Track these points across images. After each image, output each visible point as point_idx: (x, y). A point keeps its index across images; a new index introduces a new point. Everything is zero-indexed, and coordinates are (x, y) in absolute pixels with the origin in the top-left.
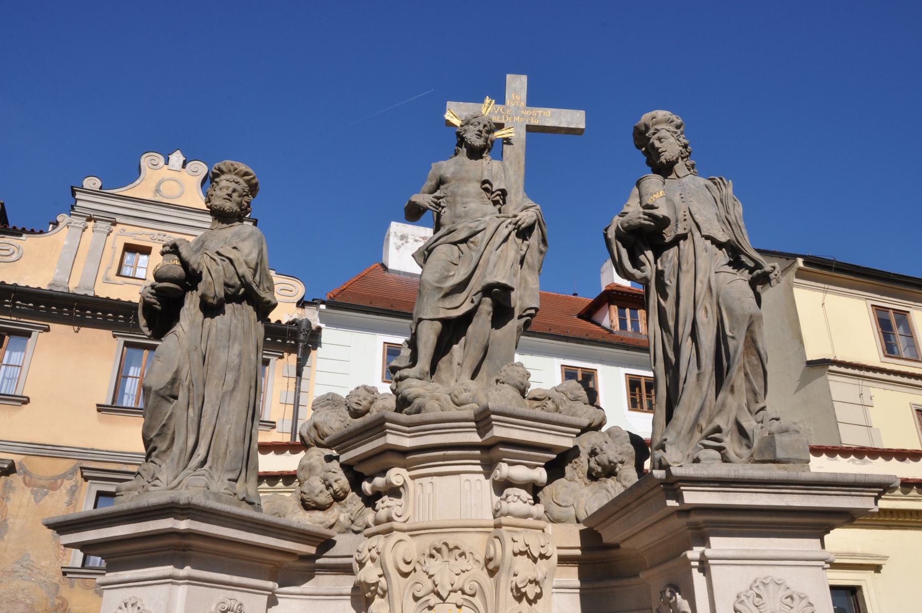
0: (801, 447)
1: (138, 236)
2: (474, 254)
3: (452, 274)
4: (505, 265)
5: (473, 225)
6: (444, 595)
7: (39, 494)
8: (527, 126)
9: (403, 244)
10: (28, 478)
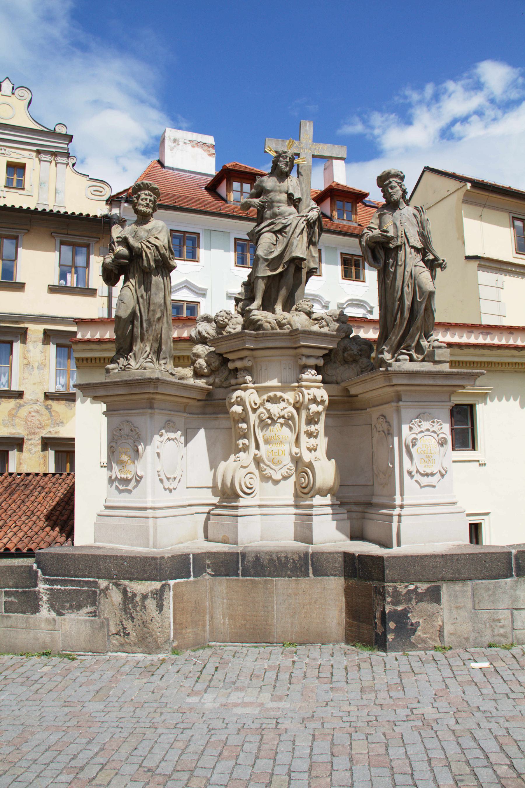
2: (285, 239)
3: (273, 250)
4: (302, 246)
5: (284, 221)
6: (276, 419)
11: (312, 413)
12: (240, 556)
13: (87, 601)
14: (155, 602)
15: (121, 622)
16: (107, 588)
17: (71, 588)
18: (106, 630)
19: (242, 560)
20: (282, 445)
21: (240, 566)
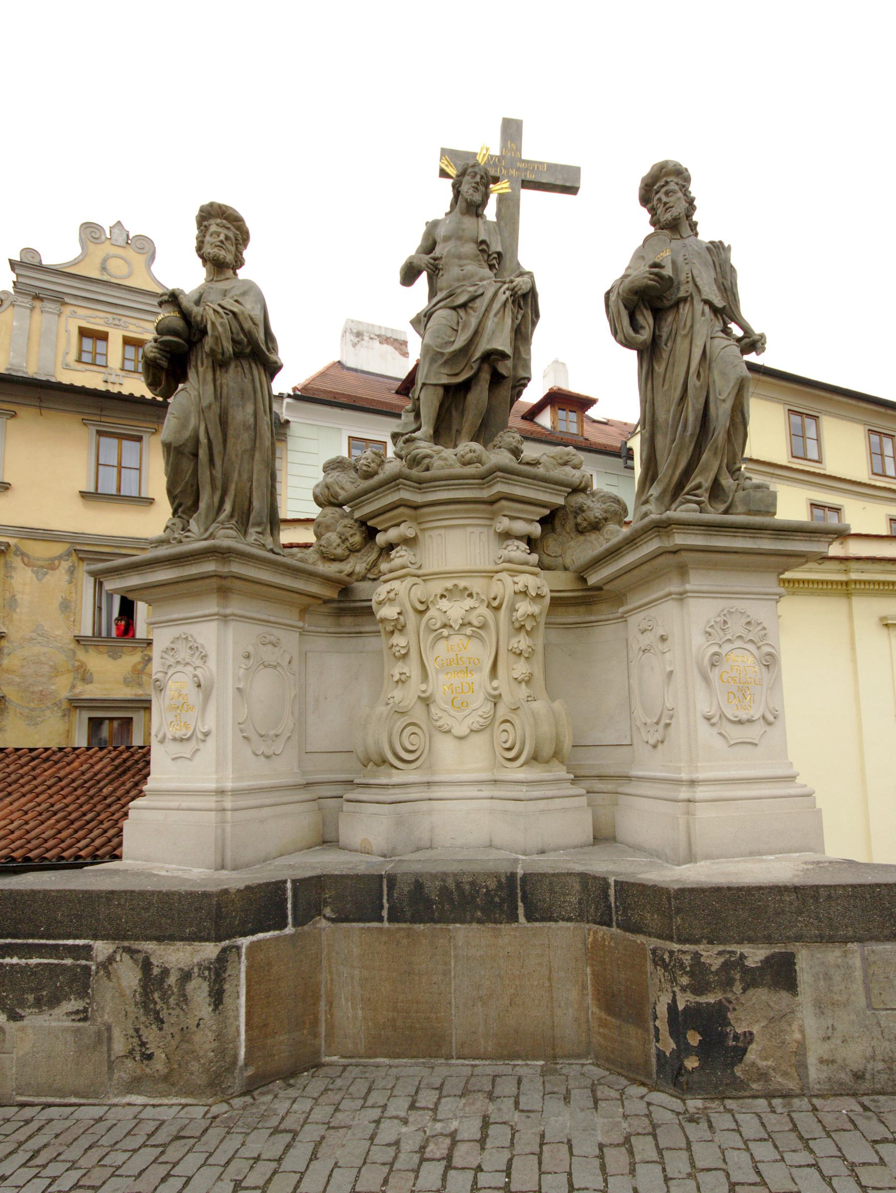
8: (523, 181)
10: (26, 559)
11: (523, 616)
12: (385, 881)
13: (71, 988)
14: (205, 986)
15: (137, 1030)
16: (111, 959)
17: (39, 961)
18: (106, 1049)
19: (389, 891)
20: (469, 675)
21: (385, 901)
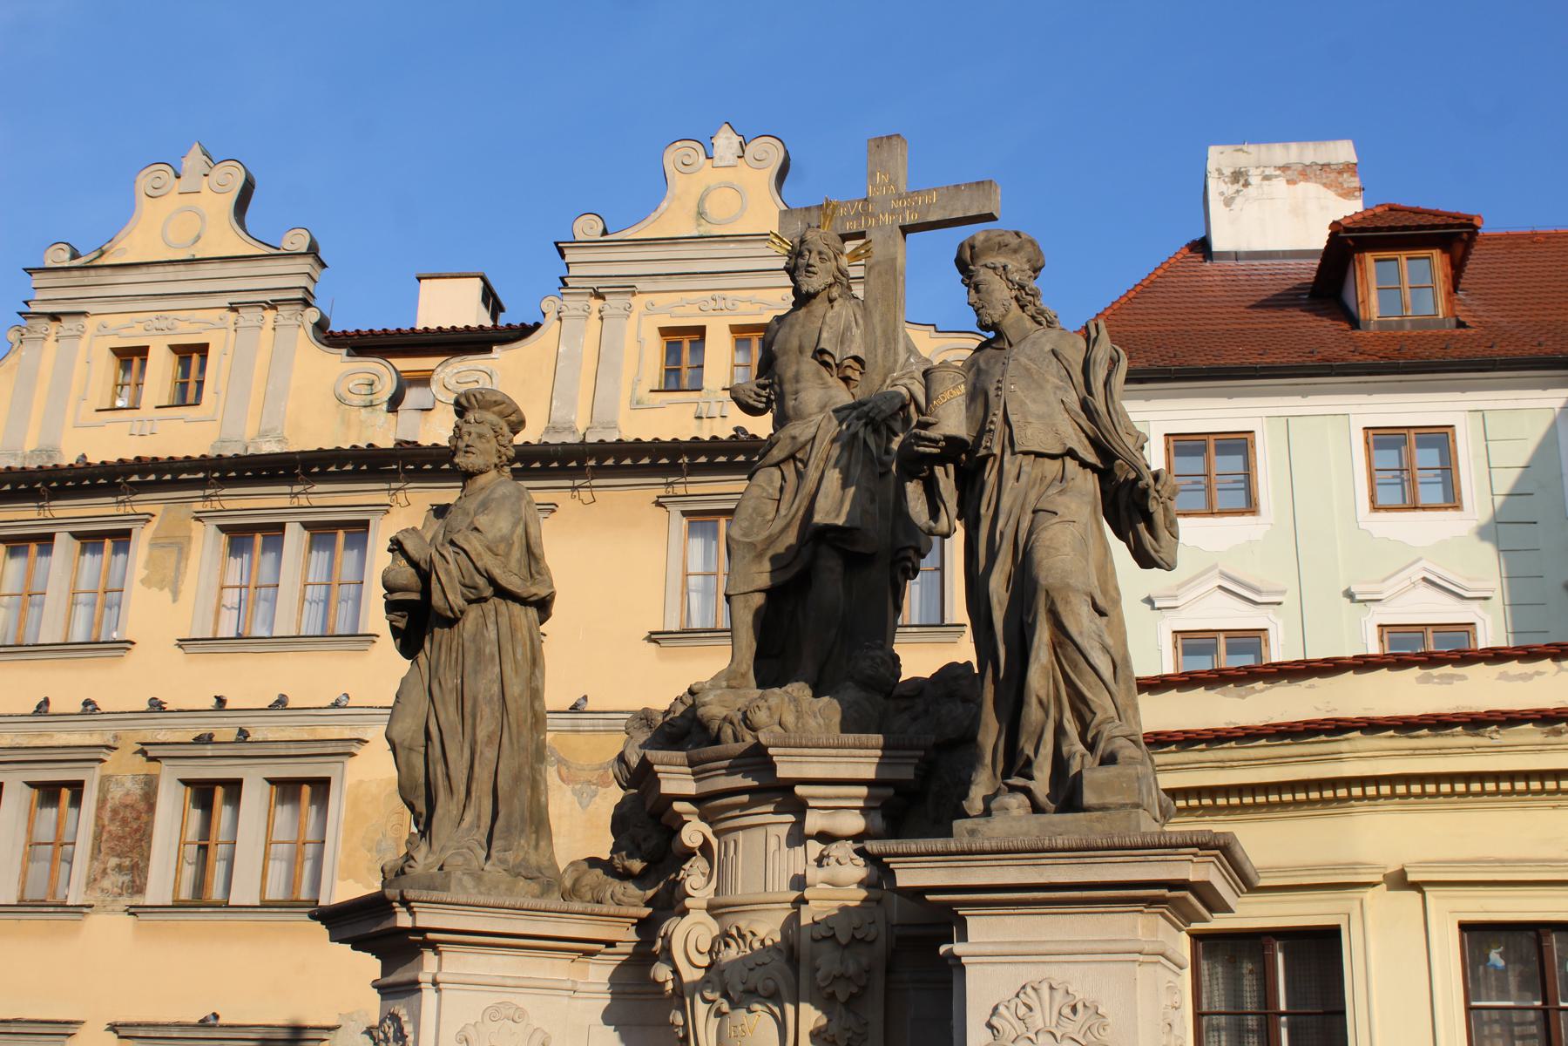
0: (1124, 785)
1: (678, 311)
7: (585, 795)
9: (1238, 192)
10: (564, 771)
